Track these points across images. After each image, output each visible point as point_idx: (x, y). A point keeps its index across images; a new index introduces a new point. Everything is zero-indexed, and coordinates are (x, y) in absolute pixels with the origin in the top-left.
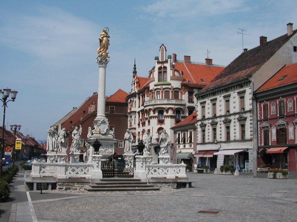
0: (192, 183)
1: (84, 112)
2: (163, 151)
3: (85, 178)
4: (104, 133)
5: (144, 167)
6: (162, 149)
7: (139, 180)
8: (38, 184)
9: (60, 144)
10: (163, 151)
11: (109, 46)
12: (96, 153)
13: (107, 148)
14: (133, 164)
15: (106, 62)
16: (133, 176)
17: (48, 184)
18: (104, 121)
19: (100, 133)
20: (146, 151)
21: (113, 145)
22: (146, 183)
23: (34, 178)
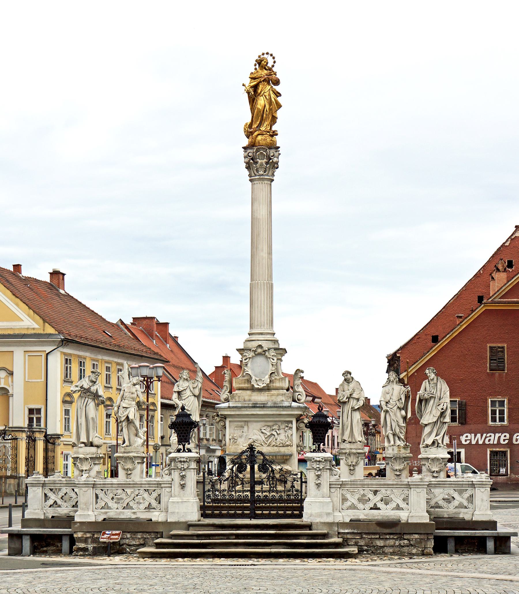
0: (512, 539)
1: (480, 299)
2: (430, 433)
3: (151, 520)
4: (262, 385)
5: (325, 488)
6: (427, 430)
7: (309, 527)
8: (34, 537)
9: (124, 424)
10: (430, 433)
11: (279, 114)
12: (181, 447)
13: (275, 433)
14: (299, 480)
15: (267, 163)
16: (300, 516)
17: (59, 538)
18: (259, 350)
19: (253, 389)
20: (391, 437)
21: (291, 422)
22: (324, 536)
23: (25, 522)
